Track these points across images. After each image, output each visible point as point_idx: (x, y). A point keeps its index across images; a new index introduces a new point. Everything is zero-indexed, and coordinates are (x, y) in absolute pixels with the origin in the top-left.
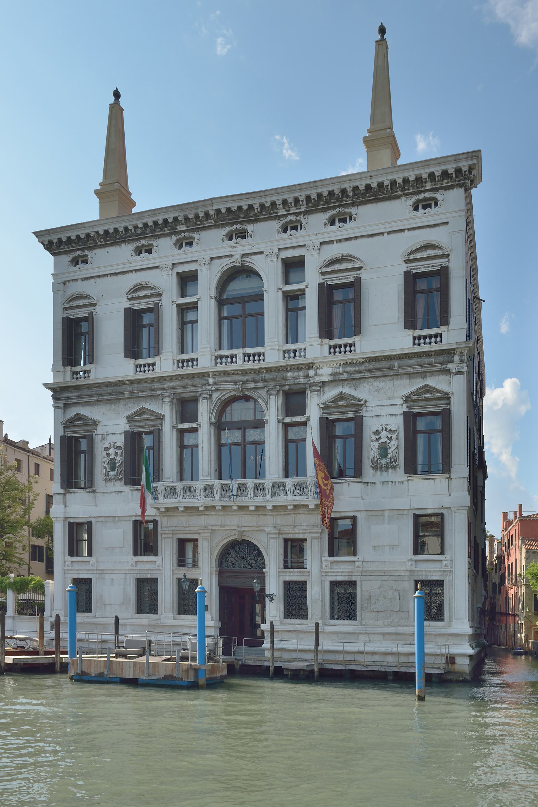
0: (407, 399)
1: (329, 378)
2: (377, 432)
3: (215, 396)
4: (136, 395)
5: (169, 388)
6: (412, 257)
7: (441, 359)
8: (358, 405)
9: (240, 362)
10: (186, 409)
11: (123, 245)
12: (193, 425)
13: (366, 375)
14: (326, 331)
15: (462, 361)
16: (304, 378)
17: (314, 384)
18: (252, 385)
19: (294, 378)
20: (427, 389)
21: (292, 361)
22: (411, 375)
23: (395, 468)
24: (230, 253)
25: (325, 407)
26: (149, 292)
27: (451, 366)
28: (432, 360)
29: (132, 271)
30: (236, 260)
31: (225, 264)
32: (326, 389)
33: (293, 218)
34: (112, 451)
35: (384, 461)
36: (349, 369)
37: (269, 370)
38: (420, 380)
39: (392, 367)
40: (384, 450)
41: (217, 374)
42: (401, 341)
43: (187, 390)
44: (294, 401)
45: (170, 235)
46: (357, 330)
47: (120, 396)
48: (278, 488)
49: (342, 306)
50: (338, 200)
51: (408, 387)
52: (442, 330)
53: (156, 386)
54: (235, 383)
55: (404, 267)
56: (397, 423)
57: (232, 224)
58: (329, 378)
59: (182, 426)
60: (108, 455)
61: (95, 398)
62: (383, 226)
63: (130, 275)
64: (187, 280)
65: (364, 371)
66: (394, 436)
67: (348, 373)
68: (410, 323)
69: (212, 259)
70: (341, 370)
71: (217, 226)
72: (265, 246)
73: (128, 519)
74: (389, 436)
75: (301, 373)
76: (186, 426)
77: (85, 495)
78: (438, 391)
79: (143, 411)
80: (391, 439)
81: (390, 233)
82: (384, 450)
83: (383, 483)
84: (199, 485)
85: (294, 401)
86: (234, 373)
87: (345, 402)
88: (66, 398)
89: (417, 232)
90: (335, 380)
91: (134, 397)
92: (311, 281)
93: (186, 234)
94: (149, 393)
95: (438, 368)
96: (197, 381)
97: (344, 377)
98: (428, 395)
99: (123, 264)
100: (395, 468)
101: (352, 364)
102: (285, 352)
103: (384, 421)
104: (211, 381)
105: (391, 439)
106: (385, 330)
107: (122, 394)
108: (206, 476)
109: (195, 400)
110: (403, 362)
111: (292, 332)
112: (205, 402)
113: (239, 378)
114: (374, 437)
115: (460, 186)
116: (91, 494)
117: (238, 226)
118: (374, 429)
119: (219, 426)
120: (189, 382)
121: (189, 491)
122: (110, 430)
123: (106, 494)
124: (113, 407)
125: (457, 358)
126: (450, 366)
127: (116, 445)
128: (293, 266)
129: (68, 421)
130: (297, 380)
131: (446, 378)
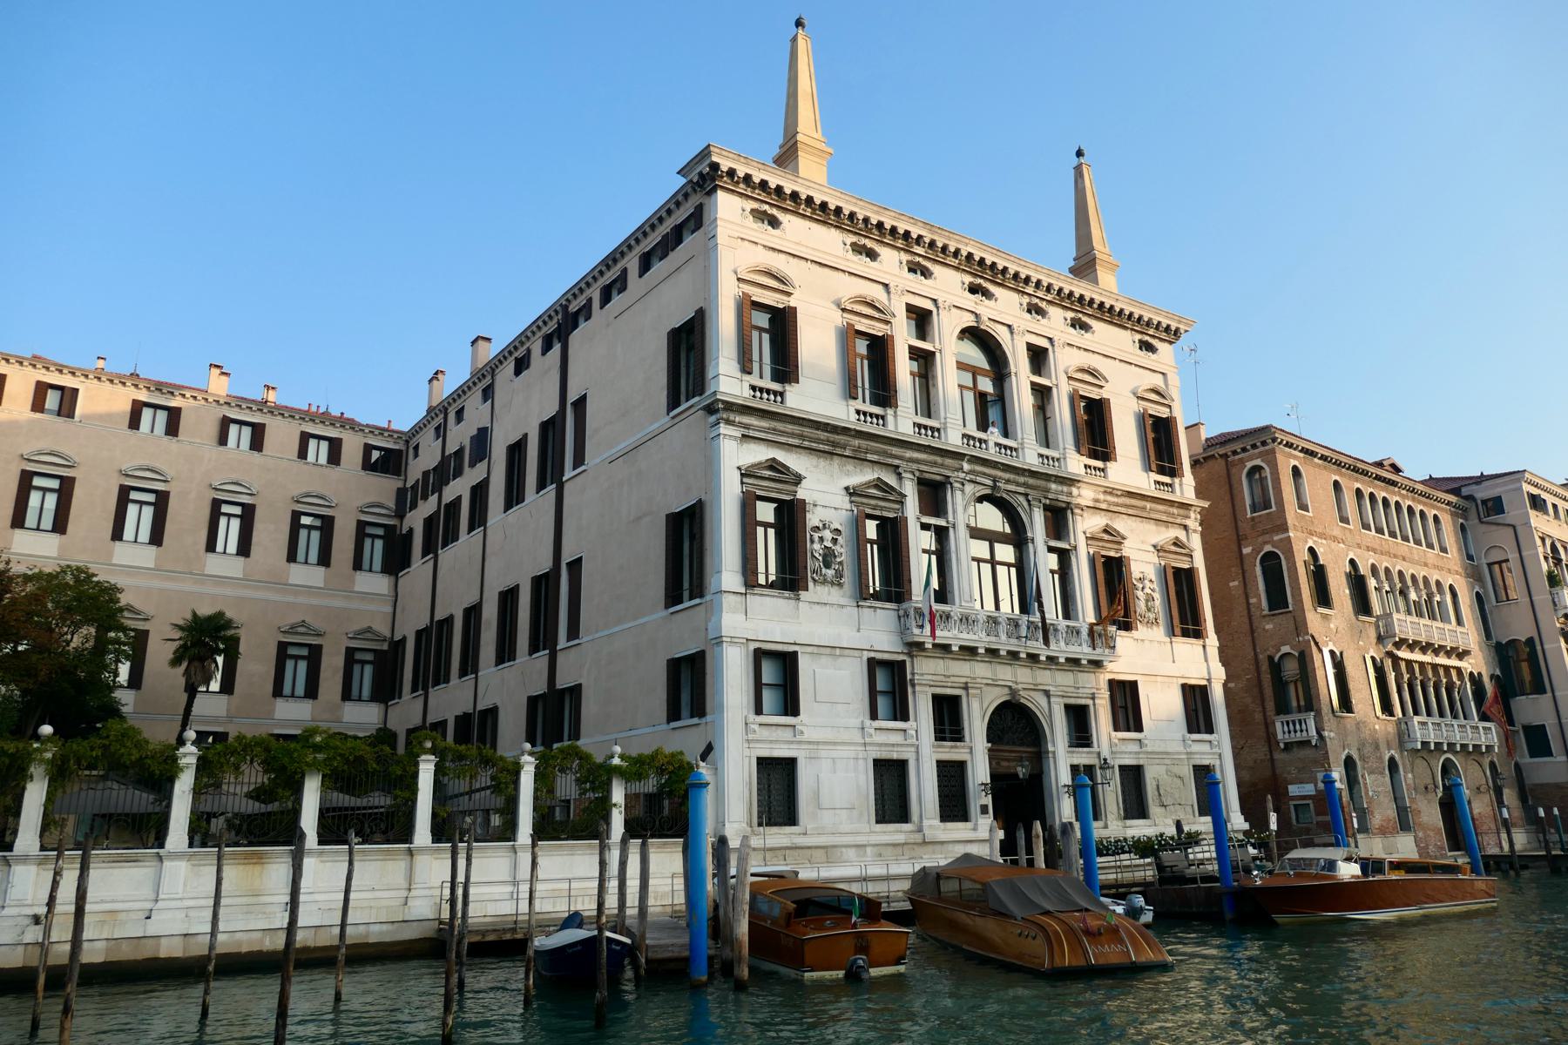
1: (1091, 504)
4: (862, 456)
5: (911, 460)
7: (1182, 512)
10: (934, 495)
19: (1057, 493)
26: (877, 315)
28: (1175, 511)
31: (969, 321)
34: (827, 535)
36: (1109, 498)
43: (934, 470)
47: (839, 451)
53: (895, 450)
57: (976, 276)
60: (821, 539)
61: (796, 442)
64: (921, 319)
67: (1109, 504)
70: (1102, 497)
71: (957, 268)
73: (857, 653)
75: (1065, 489)
77: (781, 602)
78: (1182, 546)
88: (747, 427)
91: (859, 458)
94: (882, 459)
96: (948, 461)
97: (1104, 506)
101: (1110, 491)
110: (1154, 506)
112: (958, 493)
113: (999, 473)
116: (792, 602)
120: (939, 459)
123: (817, 607)
127: (833, 527)
128: (1038, 357)
129: (753, 466)
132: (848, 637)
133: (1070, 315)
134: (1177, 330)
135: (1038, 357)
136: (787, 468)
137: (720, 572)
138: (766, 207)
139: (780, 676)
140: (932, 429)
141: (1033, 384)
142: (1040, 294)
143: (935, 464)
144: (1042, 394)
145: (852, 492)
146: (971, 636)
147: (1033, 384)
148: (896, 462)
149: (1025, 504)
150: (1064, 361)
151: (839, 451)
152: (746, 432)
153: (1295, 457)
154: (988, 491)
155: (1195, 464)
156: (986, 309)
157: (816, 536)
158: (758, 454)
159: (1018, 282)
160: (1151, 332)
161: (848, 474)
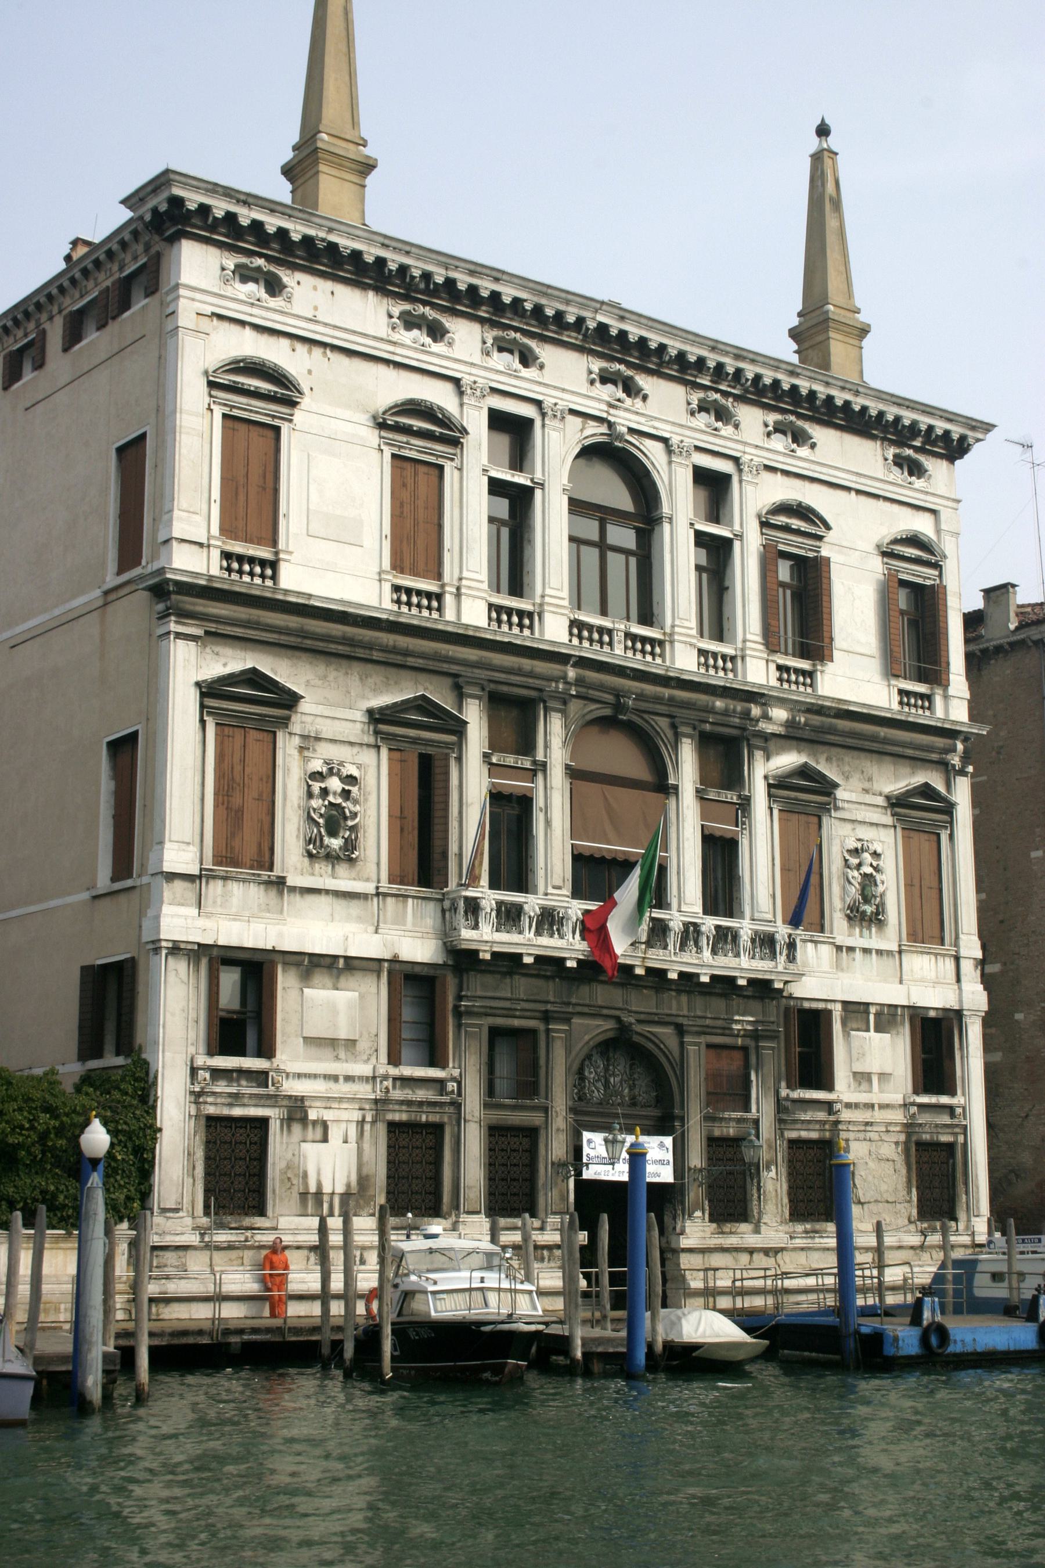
0: (897, 803)
2: (856, 852)
3: (574, 706)
4: (399, 659)
6: (900, 549)
9: (619, 650)
11: (371, 294)
16: (740, 718)
19: (726, 713)
20: (926, 791)
24: (604, 415)
25: (777, 786)
29: (387, 362)
31: (595, 432)
33: (717, 396)
34: (335, 784)
35: (869, 909)
38: (908, 770)
41: (583, 662)
45: (482, 321)
47: (360, 653)
48: (691, 933)
57: (611, 359)
58: (781, 729)
60: (325, 792)
62: (854, 478)
63: (382, 369)
69: (572, 412)
74: (875, 864)
79: (423, 705)
81: (859, 492)
83: (866, 951)
84: (532, 903)
89: (896, 508)
93: (518, 335)
94: (431, 665)
95: (934, 756)
99: (375, 338)
101: (818, 710)
107: (364, 648)
108: (559, 888)
111: (717, 620)
114: (854, 861)
117: (622, 367)
118: (852, 844)
122: (327, 729)
124: (332, 674)
127: (344, 772)
128: (714, 487)
130: (732, 719)
132: (365, 943)
133: (773, 418)
134: (963, 438)
135: (714, 487)
136: (275, 683)
137: (161, 843)
138: (260, 262)
139: (246, 1000)
140: (521, 614)
141: (698, 534)
143: (519, 672)
144: (716, 553)
145: (377, 717)
147: (698, 534)
148: (454, 669)
149: (670, 733)
150: (754, 497)
151: (360, 653)
152: (212, 627)
154: (607, 712)
155: (974, 662)
157: (316, 787)
158: (230, 662)
159: (683, 369)
160: (917, 443)
161: (376, 691)
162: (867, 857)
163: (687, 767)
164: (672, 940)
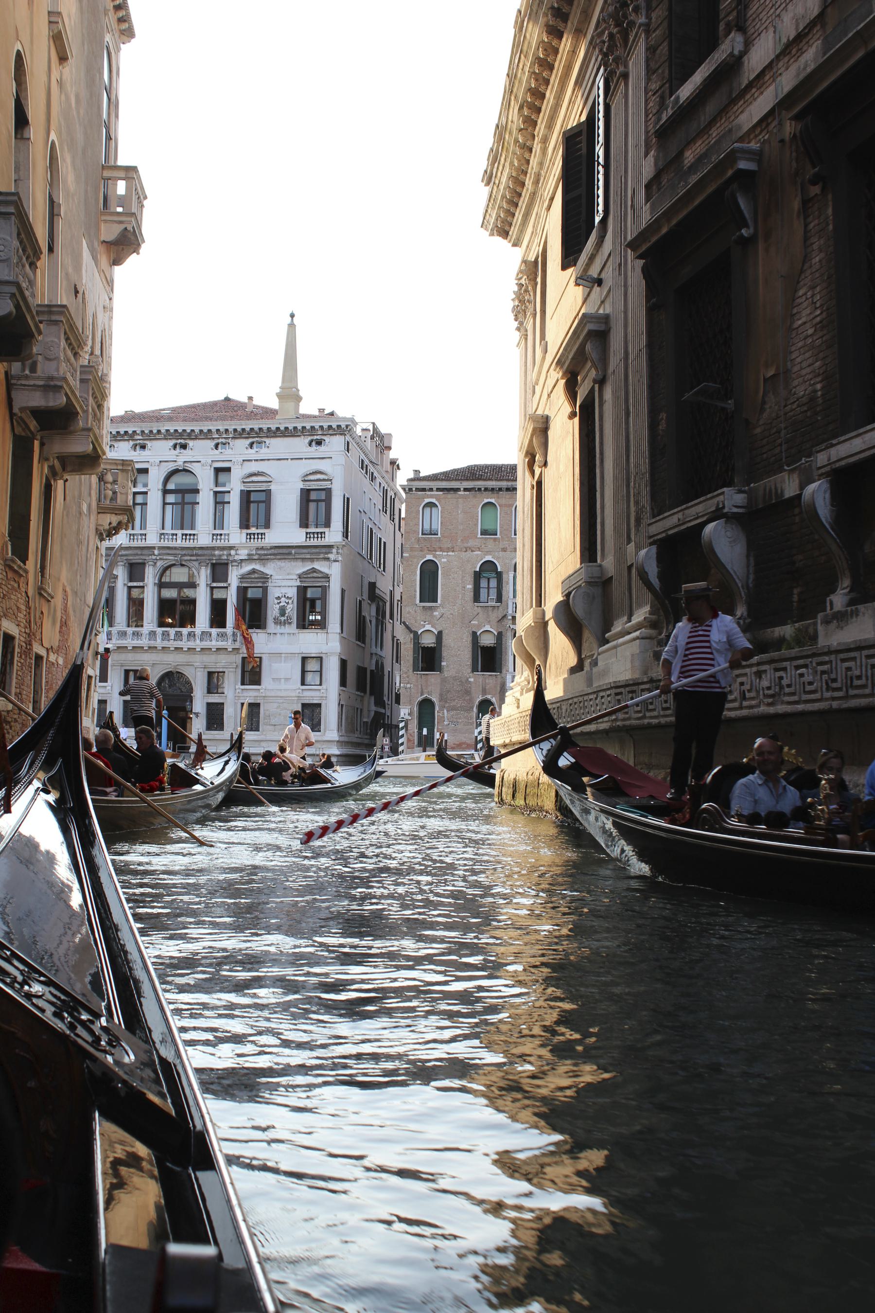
1: (246, 557)
2: (278, 598)
7: (324, 550)
8: (265, 578)
9: (179, 541)
12: (141, 584)
13: (272, 557)
14: (245, 523)
15: (338, 553)
17: (235, 561)
18: (189, 558)
19: (220, 556)
20: (314, 570)
21: (218, 543)
22: (303, 560)
23: (290, 623)
25: (242, 578)
27: (332, 556)
30: (180, 464)
31: (171, 467)
32: (243, 564)
35: (283, 619)
36: (259, 552)
37: (201, 548)
39: (290, 554)
40: (283, 612)
41: (160, 548)
42: (297, 537)
44: (219, 571)
46: (267, 525)
48: (205, 635)
49: (255, 507)
50: (257, 433)
51: (302, 568)
52: (326, 530)
54: (175, 555)
55: (301, 485)
56: (293, 593)
59: (130, 584)
65: (270, 555)
66: (290, 601)
68: (304, 523)
70: (254, 552)
72: (201, 456)
75: (225, 552)
76: (135, 584)
78: (321, 572)
80: (288, 603)
82: (283, 612)
85: (219, 571)
86: (175, 548)
87: (256, 575)
90: (250, 559)
92: (235, 486)
95: (322, 556)
96: (146, 552)
98: (315, 575)
100: (290, 623)
101: (262, 548)
102: (213, 535)
103: (284, 590)
104: (156, 552)
105: (288, 603)
106: (286, 529)
109: (143, 565)
111: (219, 522)
112: (151, 567)
114: (276, 601)
115: (341, 434)
119: (161, 585)
121: (136, 635)
125: (334, 550)
126: (330, 556)
131: (327, 563)
142: (225, 436)
143: (137, 555)
146: (139, 642)
153: (428, 497)
156: (181, 458)
162: (283, 599)
163: (203, 577)
164: (185, 638)
